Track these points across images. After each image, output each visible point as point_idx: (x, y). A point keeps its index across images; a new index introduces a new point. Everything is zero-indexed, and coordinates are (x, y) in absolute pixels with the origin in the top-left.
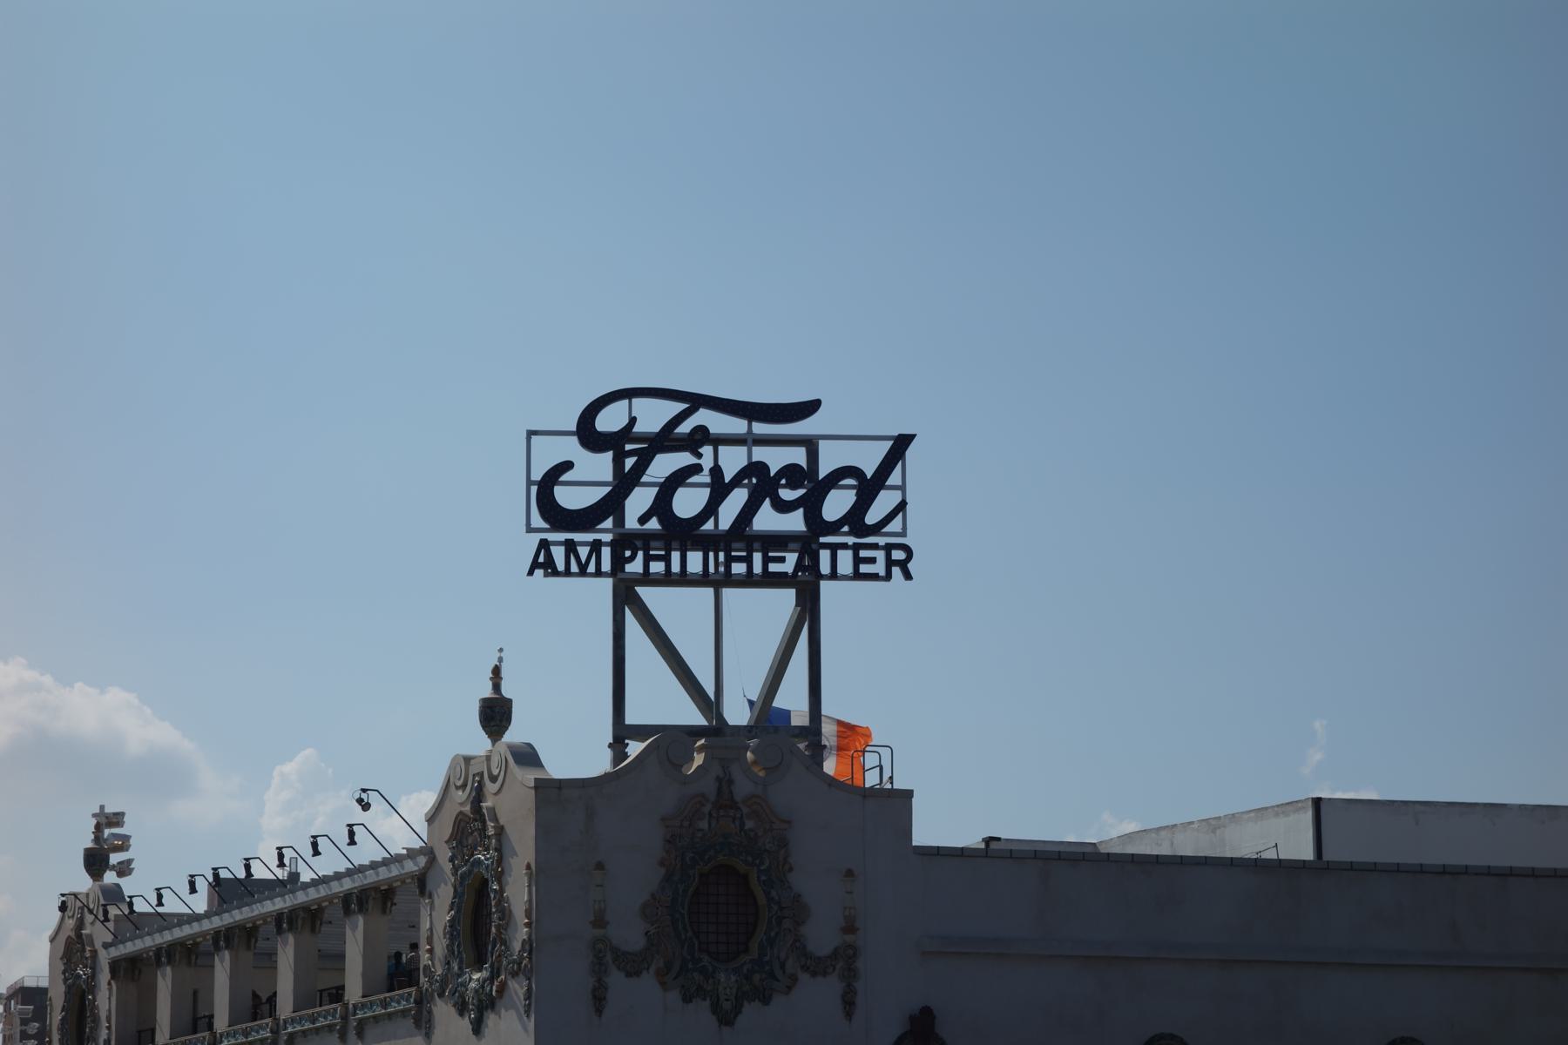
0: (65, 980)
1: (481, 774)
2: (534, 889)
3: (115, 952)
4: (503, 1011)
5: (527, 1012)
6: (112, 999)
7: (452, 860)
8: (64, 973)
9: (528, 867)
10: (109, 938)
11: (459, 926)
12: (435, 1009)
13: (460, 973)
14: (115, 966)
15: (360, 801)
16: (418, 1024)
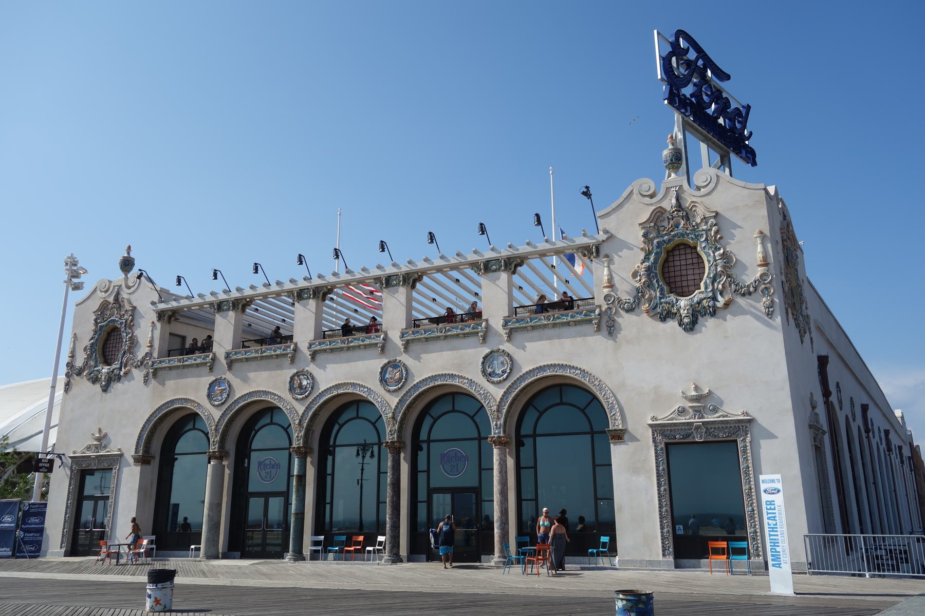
0: (96, 323)
1: (681, 187)
2: (769, 246)
3: (162, 306)
4: (729, 317)
5: (770, 314)
6: (155, 331)
7: (645, 235)
8: (96, 320)
9: (761, 233)
10: (156, 299)
11: (656, 270)
12: (619, 320)
13: (662, 296)
14: (161, 315)
15: (584, 193)
16: (599, 329)
